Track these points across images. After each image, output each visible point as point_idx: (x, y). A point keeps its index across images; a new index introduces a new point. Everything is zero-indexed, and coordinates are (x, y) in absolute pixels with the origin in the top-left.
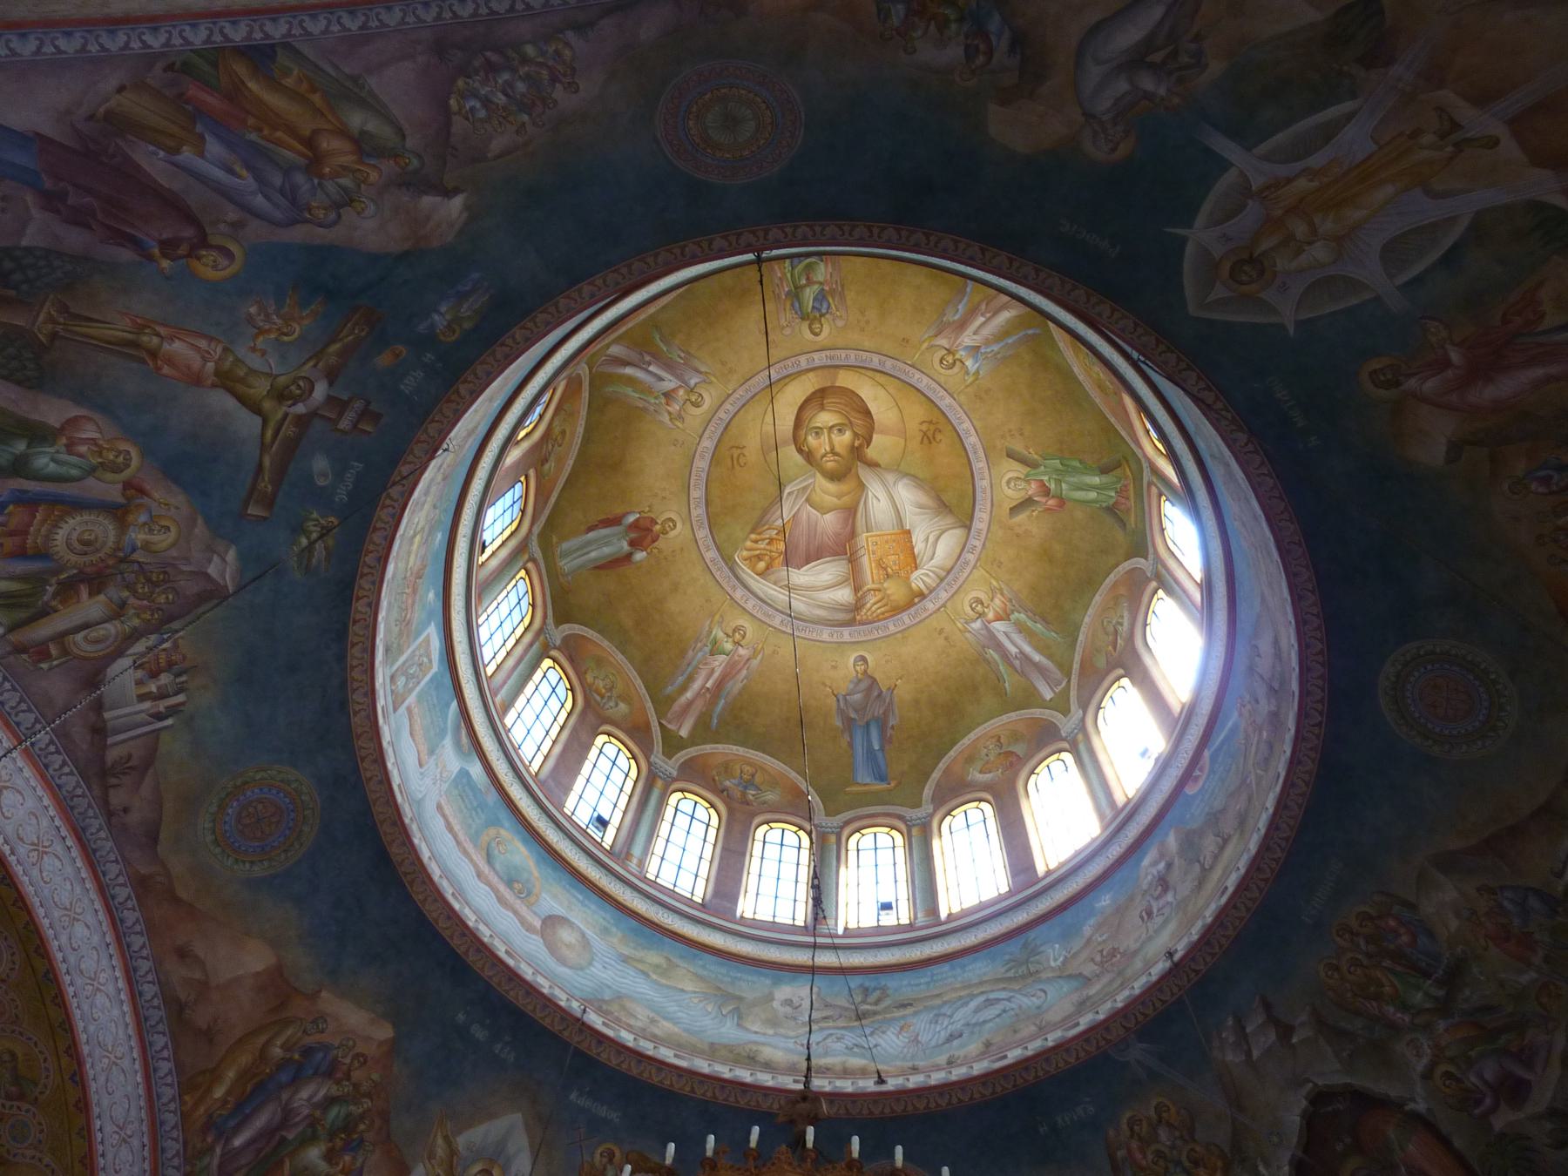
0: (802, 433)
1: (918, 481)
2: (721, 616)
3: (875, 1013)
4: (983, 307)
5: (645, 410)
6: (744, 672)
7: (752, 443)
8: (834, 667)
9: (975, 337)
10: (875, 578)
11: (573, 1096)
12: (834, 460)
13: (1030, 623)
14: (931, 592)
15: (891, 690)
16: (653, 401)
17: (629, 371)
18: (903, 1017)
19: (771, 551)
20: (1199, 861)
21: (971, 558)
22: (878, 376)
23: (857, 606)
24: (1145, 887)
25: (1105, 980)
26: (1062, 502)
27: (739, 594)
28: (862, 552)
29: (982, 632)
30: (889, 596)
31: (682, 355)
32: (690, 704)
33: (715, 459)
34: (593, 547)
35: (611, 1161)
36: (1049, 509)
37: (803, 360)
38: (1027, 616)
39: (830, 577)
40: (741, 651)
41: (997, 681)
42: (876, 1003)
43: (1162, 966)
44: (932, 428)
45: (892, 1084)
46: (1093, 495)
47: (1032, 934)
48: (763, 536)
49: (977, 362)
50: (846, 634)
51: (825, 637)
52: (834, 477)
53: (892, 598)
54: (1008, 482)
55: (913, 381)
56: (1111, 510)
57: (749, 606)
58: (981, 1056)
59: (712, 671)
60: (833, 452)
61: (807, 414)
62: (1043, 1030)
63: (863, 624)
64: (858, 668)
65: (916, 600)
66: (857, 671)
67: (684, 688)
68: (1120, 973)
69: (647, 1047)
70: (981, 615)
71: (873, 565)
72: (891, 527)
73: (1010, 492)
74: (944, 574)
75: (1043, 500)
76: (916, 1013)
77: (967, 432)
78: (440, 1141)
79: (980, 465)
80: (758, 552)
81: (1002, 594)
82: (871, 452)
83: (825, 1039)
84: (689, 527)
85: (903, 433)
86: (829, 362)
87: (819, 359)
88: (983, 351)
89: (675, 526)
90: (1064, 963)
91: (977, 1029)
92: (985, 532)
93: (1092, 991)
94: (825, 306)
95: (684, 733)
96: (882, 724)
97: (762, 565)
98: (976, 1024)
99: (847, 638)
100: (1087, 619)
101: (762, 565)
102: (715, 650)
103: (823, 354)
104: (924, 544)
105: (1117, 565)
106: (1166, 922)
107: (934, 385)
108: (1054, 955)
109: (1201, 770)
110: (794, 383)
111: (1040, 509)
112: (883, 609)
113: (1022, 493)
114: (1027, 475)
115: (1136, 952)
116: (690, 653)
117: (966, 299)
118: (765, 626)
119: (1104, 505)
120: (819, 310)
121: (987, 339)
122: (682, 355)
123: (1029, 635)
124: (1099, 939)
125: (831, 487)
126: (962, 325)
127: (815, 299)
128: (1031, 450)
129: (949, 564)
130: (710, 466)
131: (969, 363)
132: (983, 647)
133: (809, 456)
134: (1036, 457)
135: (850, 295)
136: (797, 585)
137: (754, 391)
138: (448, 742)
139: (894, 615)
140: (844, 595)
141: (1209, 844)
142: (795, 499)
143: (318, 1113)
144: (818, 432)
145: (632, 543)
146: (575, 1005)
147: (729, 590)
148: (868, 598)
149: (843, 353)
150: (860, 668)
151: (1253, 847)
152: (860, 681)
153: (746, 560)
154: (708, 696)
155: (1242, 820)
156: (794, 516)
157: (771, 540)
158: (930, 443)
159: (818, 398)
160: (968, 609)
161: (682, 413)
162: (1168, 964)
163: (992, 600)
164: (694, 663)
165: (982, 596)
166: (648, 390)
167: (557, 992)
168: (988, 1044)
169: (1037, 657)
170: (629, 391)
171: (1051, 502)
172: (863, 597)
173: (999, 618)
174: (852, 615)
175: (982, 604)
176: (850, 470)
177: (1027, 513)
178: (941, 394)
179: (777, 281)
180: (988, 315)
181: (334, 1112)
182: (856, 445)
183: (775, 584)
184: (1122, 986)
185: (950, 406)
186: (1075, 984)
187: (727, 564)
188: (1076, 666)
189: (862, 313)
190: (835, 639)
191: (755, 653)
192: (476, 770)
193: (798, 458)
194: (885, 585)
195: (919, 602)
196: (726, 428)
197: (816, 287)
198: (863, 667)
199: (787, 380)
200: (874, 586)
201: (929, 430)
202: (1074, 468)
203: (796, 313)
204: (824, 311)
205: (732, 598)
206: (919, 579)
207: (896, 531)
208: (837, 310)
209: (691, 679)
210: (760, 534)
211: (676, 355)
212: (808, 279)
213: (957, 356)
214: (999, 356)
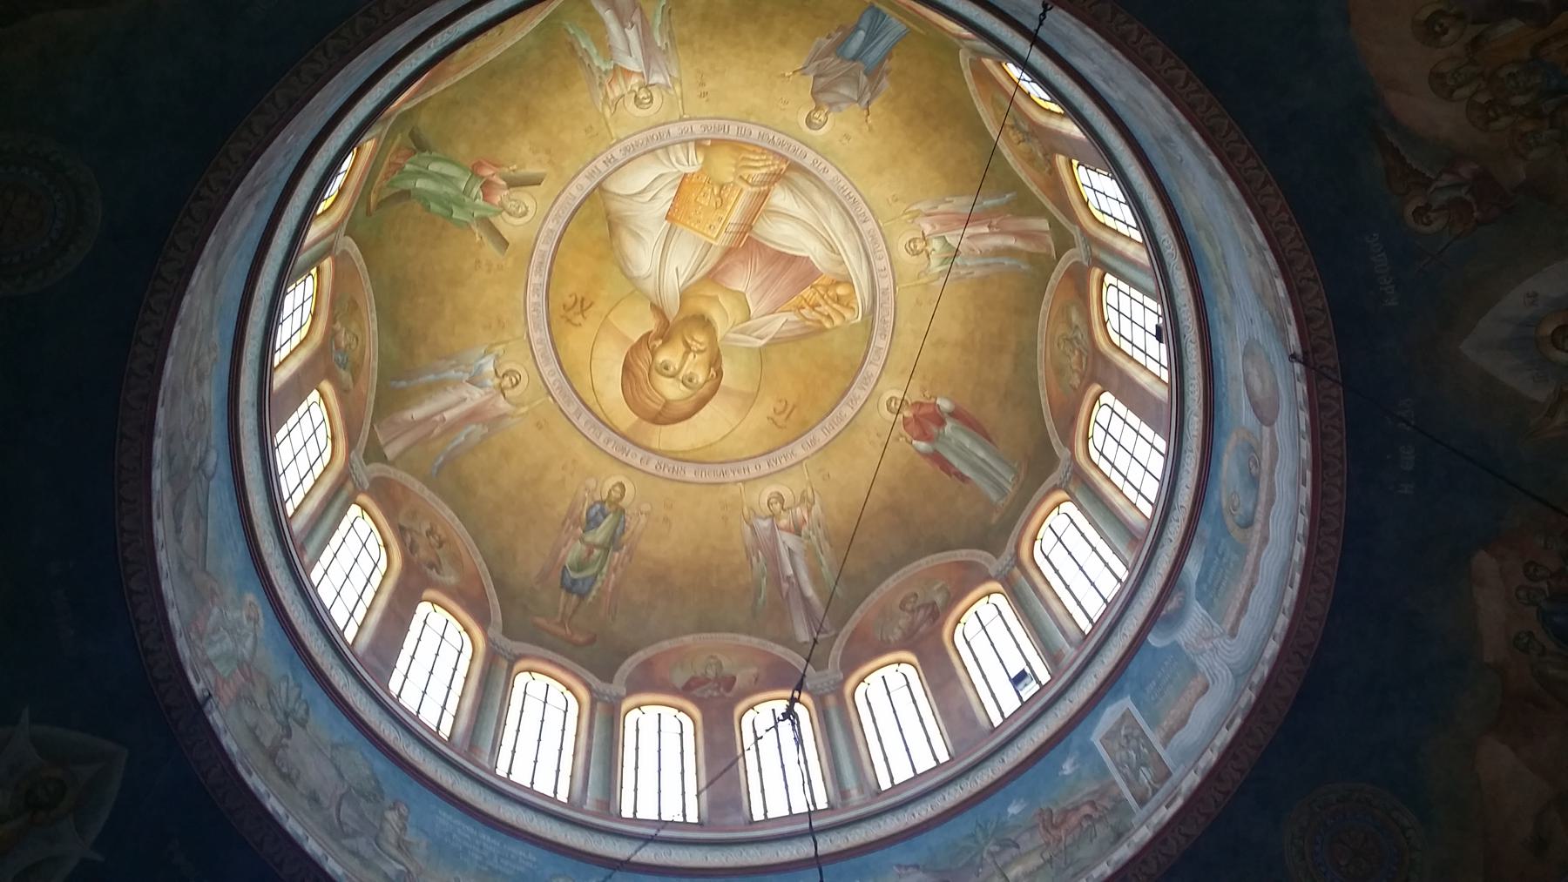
0: (705, 390)
1: (623, 265)
2: (919, 278)
4: (437, 431)
5: (827, 537)
6: (942, 208)
7: (759, 415)
8: (847, 137)
9: (467, 395)
10: (736, 193)
12: (693, 339)
13: (593, 51)
14: (686, 142)
15: (803, 71)
16: (814, 538)
17: (810, 592)
19: (822, 297)
21: (617, 152)
22: (591, 402)
23: (777, 178)
26: (475, 171)
27: (885, 283)
28: (731, 228)
29: (656, 68)
30: (736, 166)
31: (754, 559)
32: (1020, 235)
33: (805, 428)
34: (975, 459)
35: (1427, 207)
36: (495, 165)
37: (651, 468)
38: (590, 58)
39: (783, 226)
40: (928, 229)
41: (673, 11)
44: (570, 314)
48: (818, 317)
49: (481, 365)
50: (809, 160)
52: (705, 323)
53: (734, 162)
54: (525, 214)
60: (688, 349)
61: (686, 407)
63: (780, 155)
64: (822, 118)
67: (1010, 252)
71: (729, 207)
72: (682, 231)
74: (659, 152)
75: (495, 178)
77: (536, 291)
79: (545, 247)
80: (835, 306)
81: (606, 96)
82: (651, 324)
85: (605, 323)
86: (628, 446)
87: (635, 457)
88: (467, 377)
89: (891, 399)
92: (585, 172)
94: (593, 512)
96: (838, 48)
97: (841, 290)
99: (811, 156)
101: (841, 290)
103: (628, 459)
104: (660, 195)
110: (674, 449)
111: (507, 170)
112: (752, 157)
113: (514, 196)
116: (978, 273)
117: (450, 447)
118: (884, 231)
119: (426, 154)
120: (602, 510)
121: (455, 388)
122: (754, 559)
125: (715, 315)
126: (472, 416)
127: (598, 524)
128: (478, 239)
129: (645, 159)
130: (813, 427)
132: (665, 52)
133: (715, 363)
134: (477, 231)
135: (563, 508)
136: (821, 242)
137: (718, 468)
139: (745, 143)
140: (781, 198)
142: (762, 327)
144: (688, 381)
145: (942, 423)
147: (892, 295)
149: (609, 448)
150: (819, 116)
152: (830, 105)
153: (853, 309)
154: (995, 222)
156: (773, 313)
158: (583, 299)
159: (666, 416)
161: (798, 500)
164: (982, 262)
165: (631, 105)
166: (811, 554)
170: (825, 570)
171: (487, 172)
172: (763, 183)
173: (628, 73)
174: (789, 173)
175: (636, 97)
176: (684, 320)
177: (522, 172)
178: (539, 347)
179: (620, 570)
180: (437, 418)
182: (660, 342)
185: (537, 327)
189: (563, 480)
190: (825, 164)
191: (917, 215)
194: (731, 179)
195: (706, 139)
196: (770, 452)
197: (589, 538)
198: (816, 115)
199: (680, 456)
200: (744, 186)
201: (575, 314)
202: (440, 203)
203: (625, 522)
204: (598, 506)
206: (690, 162)
207: (680, 226)
208: (585, 499)
209: (998, 252)
210: (819, 322)
211: (759, 562)
212: (590, 553)
213: (497, 381)
214: (454, 362)
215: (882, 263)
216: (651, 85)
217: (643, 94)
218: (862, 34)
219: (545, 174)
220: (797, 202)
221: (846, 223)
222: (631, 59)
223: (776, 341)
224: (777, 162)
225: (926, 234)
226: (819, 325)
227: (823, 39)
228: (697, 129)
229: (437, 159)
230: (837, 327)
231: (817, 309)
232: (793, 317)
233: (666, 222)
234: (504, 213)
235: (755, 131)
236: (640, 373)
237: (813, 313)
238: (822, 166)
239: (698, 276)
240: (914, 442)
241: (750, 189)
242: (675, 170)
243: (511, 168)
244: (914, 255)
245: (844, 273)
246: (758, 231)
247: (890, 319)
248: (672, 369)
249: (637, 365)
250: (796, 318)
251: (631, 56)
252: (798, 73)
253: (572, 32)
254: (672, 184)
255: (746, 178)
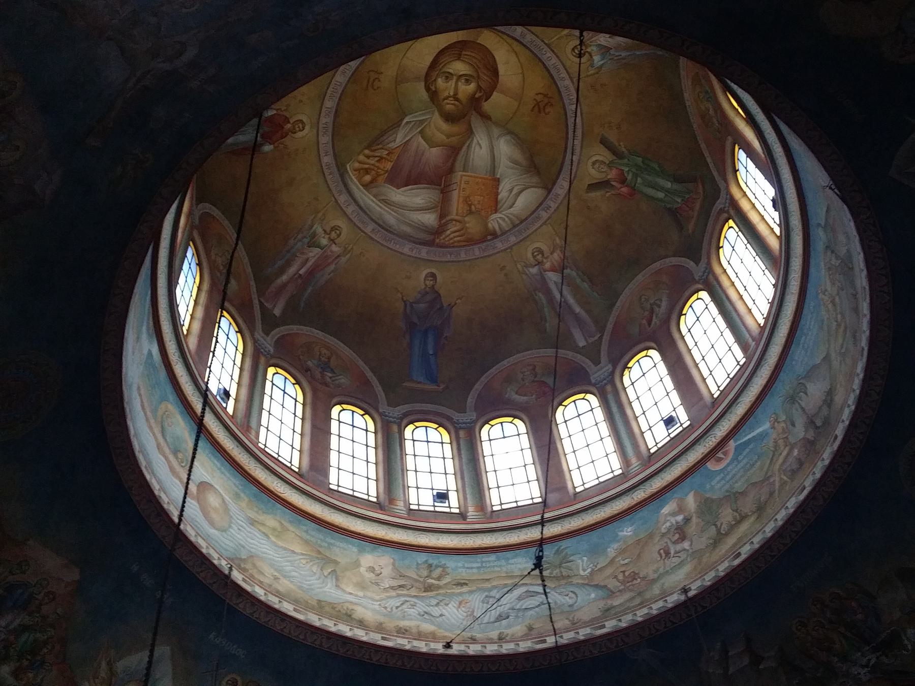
0: (434, 74)
1: (519, 141)
2: (324, 214)
3: (439, 587)
6: (332, 267)
11: (212, 636)
13: (578, 281)
14: (504, 233)
15: (451, 307)
18: (461, 594)
19: (378, 168)
20: (715, 525)
21: (545, 215)
23: (439, 231)
24: (663, 531)
25: (627, 595)
26: (633, 190)
27: (343, 199)
28: (454, 187)
30: (467, 228)
32: (284, 286)
38: (578, 274)
39: (423, 201)
40: (335, 248)
42: (439, 579)
43: (675, 598)
44: (546, 100)
45: (456, 649)
46: (661, 195)
47: (564, 544)
49: (602, 60)
50: (424, 252)
51: (406, 250)
52: (449, 118)
54: (594, 163)
55: (544, 58)
56: (674, 213)
57: (349, 210)
58: (525, 637)
59: (307, 260)
60: (456, 98)
62: (575, 625)
63: (441, 247)
64: (428, 283)
65: (489, 237)
66: (426, 285)
67: (282, 271)
68: (640, 594)
69: (274, 601)
70: (539, 263)
73: (593, 172)
74: (518, 222)
76: (471, 592)
78: (104, 664)
80: (367, 166)
82: (487, 106)
83: (402, 604)
84: (315, 131)
88: (612, 52)
89: (304, 128)
90: (592, 573)
91: (520, 614)
93: (617, 602)
95: (277, 312)
97: (368, 178)
98: (519, 610)
100: (627, 290)
101: (368, 178)
102: (313, 244)
105: (666, 257)
106: (681, 564)
107: (560, 66)
108: (582, 565)
109: (725, 454)
111: (613, 192)
114: (611, 162)
115: (654, 581)
116: (292, 242)
119: (669, 206)
123: (576, 291)
124: (622, 562)
125: (445, 126)
131: (596, 58)
133: (433, 95)
134: (624, 150)
136: (393, 202)
138: (144, 329)
139: (468, 245)
140: (430, 219)
141: (727, 515)
142: (410, 129)
143: (12, 638)
144: (448, 76)
146: (224, 563)
148: (450, 226)
150: (430, 283)
151: (769, 530)
154: (300, 281)
155: (760, 509)
156: (405, 143)
157: (381, 159)
158: (539, 112)
160: (530, 255)
162: (683, 598)
163: (552, 253)
165: (544, 248)
167: (212, 552)
168: (530, 628)
169: (578, 309)
172: (446, 224)
173: (553, 269)
175: (543, 255)
177: (602, 192)
181: (24, 638)
182: (477, 96)
183: (375, 196)
184: (642, 605)
186: (601, 593)
187: (339, 170)
188: (610, 326)
192: (155, 350)
193: (424, 95)
194: (466, 219)
201: (542, 101)
205: (336, 201)
206: (496, 221)
209: (288, 264)
210: (372, 151)
214: (624, 61)
215: (350, 209)
216: (536, 265)
217: (539, 257)
218: (431, 352)
219: (587, 192)
220: (420, 221)
221: (384, 222)
222: (556, 280)
223: (397, 125)
224: (442, 241)
225: (334, 245)
226: (373, 148)
227: (447, 335)
228: (499, 245)
229: (660, 200)
230: (359, 154)
231: (378, 158)
232: (393, 145)
233: (498, 176)
234: (608, 162)
235: (463, 256)
236: (485, 72)
237: (379, 154)
238: (414, 252)
239: (465, 148)
240: (275, 112)
241: (452, 217)
242: (503, 213)
243: (609, 194)
244: (334, 226)
245: (371, 190)
246: (437, 191)
247: (329, 177)
248: (463, 81)
249: (487, 76)
250: (390, 145)
251: (555, 282)
252: (453, 304)
253: (595, 293)
254: (503, 202)
255: (458, 223)
